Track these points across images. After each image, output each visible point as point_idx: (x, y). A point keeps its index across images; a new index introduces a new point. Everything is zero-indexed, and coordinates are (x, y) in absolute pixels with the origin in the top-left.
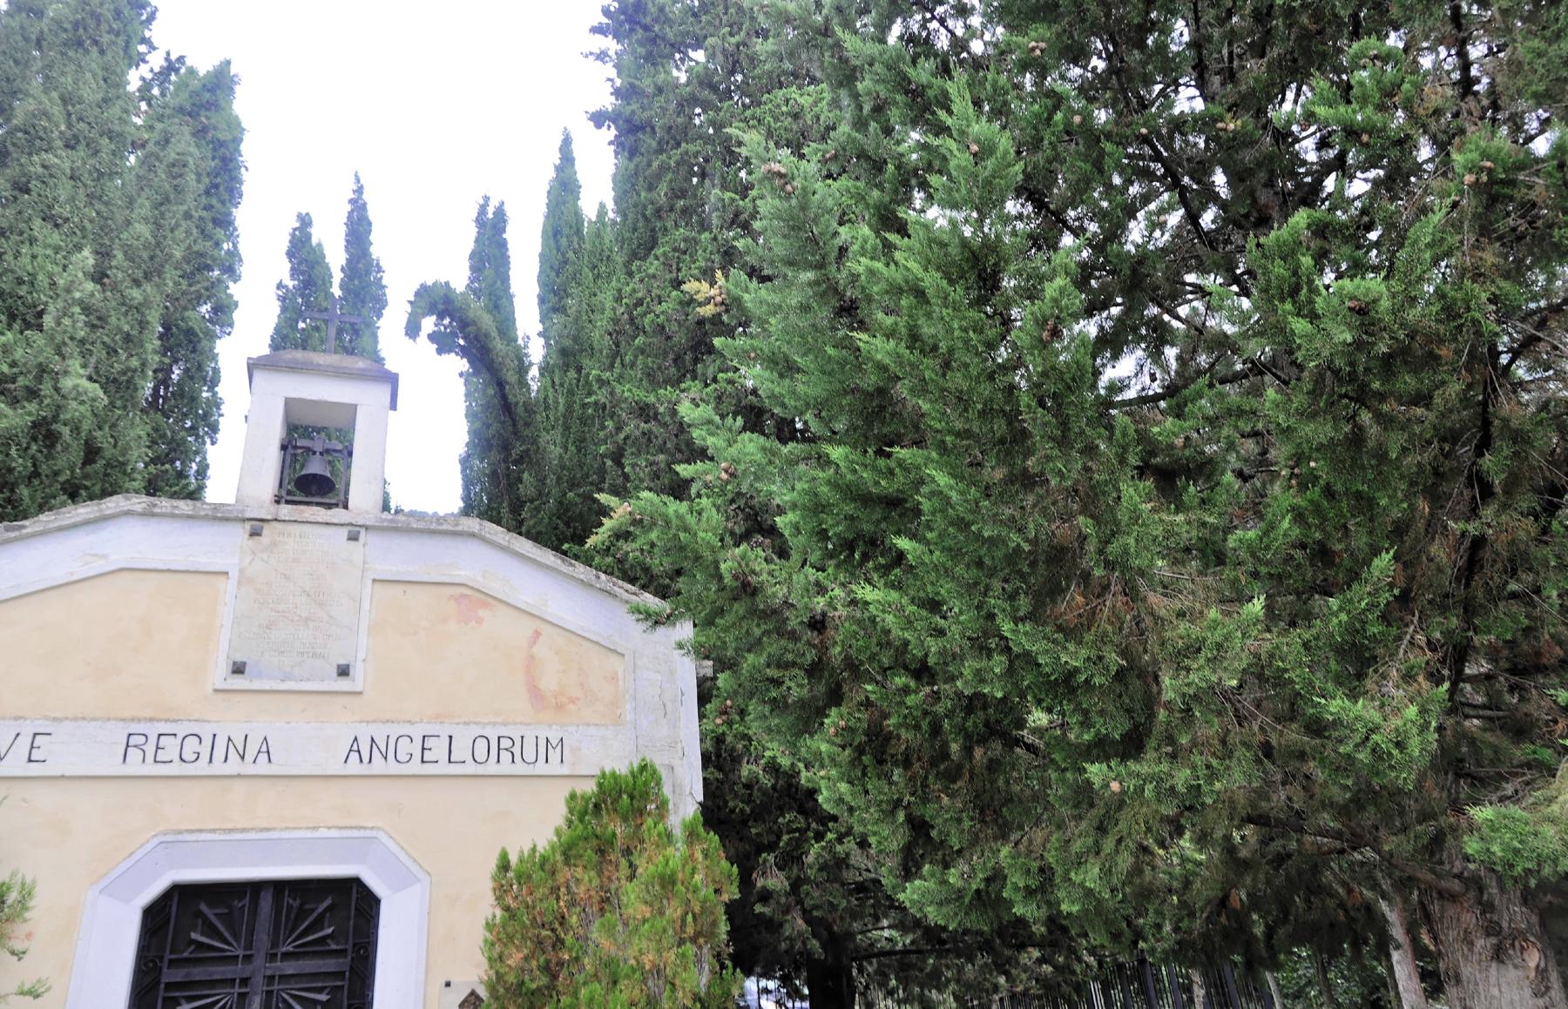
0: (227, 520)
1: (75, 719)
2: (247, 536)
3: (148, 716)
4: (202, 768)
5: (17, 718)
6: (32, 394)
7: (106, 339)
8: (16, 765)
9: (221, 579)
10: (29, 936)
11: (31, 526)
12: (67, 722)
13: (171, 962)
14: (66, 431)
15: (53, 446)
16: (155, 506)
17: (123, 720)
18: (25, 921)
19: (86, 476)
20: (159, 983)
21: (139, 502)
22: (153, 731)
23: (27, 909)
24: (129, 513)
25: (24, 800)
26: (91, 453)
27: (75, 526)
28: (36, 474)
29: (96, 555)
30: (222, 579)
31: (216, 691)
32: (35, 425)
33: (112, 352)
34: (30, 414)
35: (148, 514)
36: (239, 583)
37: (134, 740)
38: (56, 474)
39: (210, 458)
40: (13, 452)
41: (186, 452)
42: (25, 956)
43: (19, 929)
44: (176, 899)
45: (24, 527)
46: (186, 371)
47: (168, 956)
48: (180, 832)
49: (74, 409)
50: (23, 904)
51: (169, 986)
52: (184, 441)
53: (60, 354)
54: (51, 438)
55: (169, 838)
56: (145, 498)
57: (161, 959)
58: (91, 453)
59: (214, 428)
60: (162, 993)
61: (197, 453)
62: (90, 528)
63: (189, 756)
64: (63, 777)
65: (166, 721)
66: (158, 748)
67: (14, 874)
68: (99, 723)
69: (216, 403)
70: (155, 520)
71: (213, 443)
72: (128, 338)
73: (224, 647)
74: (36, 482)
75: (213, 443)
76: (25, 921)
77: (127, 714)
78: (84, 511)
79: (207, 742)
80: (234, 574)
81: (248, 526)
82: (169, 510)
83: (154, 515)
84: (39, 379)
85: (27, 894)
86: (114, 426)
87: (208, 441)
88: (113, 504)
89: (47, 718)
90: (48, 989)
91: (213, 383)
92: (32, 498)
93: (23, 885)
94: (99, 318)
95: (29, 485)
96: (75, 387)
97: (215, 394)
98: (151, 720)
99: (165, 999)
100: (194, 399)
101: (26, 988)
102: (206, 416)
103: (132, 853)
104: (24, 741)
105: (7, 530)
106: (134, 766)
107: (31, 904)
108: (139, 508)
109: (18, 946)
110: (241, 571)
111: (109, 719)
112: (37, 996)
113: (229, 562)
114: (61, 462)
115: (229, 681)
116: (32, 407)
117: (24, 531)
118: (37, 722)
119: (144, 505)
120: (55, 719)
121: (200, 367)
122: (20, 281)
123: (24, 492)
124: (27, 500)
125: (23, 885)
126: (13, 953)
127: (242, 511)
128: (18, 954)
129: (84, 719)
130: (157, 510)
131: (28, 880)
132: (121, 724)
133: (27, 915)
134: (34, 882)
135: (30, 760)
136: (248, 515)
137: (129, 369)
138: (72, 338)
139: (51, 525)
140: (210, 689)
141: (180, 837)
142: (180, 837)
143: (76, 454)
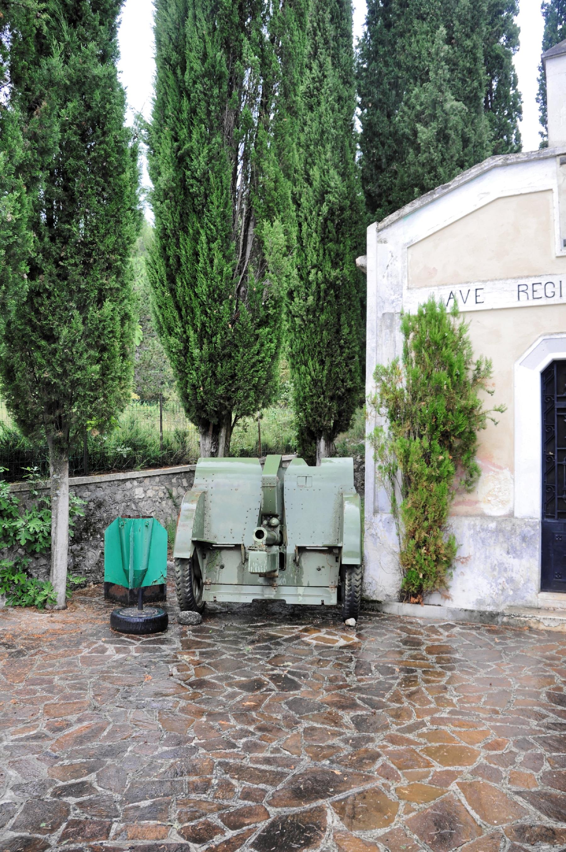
0: (546, 158)
1: (492, 280)
2: (559, 165)
3: (526, 274)
4: (556, 300)
5: (467, 283)
6: (434, 117)
7: (460, 75)
8: (471, 305)
9: (548, 195)
10: (493, 384)
11: (452, 184)
12: (489, 282)
13: (558, 398)
14: (452, 132)
15: (447, 143)
16: (508, 159)
17: (514, 278)
18: (491, 378)
19: (466, 155)
20: (554, 408)
21: (499, 159)
22: (529, 282)
23: (490, 372)
24: (495, 167)
25: (478, 322)
26: (466, 141)
27: (471, 180)
28: (444, 160)
29: (485, 193)
30: (549, 193)
31: (557, 257)
32: (438, 133)
33: (464, 81)
34: (434, 128)
35: (505, 165)
36: (559, 194)
37: (522, 288)
38: (452, 157)
39: (521, 131)
40: (432, 151)
41: (508, 130)
42: (494, 394)
43: (488, 381)
44: (555, 369)
45: (449, 186)
46: (499, 82)
47: (556, 396)
48: (552, 334)
49: (454, 119)
50: (488, 370)
51: (559, 410)
52: (506, 123)
53: (441, 91)
54: (446, 138)
55: (548, 337)
56: (501, 157)
57: (553, 396)
58: (466, 141)
59: (520, 111)
60: (556, 413)
61: (514, 128)
62: (478, 179)
63: (549, 294)
64: (492, 309)
65: (535, 276)
66: (534, 291)
67: (481, 356)
68: (504, 281)
69: (518, 96)
70: (509, 167)
71: (521, 120)
72: (470, 71)
73: (557, 232)
74: (444, 163)
75: (521, 120)
76: (491, 378)
77: (515, 275)
78: (474, 171)
79: (557, 285)
80: (555, 190)
81: (558, 159)
82: (515, 160)
83: (508, 165)
84: (434, 108)
85: (489, 366)
86: (472, 122)
87: (518, 119)
88: (488, 163)
89: (479, 281)
90: (506, 409)
91: (515, 83)
92: (445, 172)
93: (486, 361)
94: (454, 65)
95: (442, 166)
96: (452, 107)
97: (516, 90)
98: (527, 277)
99: (558, 416)
100: (506, 96)
101: (497, 408)
102: (515, 104)
103: (531, 346)
104: (472, 293)
105: (443, 188)
106: (524, 302)
107: (492, 370)
108: (500, 163)
109: (490, 389)
110: (559, 187)
111: (507, 279)
112: (502, 412)
113: (552, 184)
114: (453, 151)
115: (563, 251)
116: (434, 124)
117: (452, 187)
118: (476, 284)
119: (502, 160)
120: (483, 281)
121: (506, 77)
122: (415, 58)
123: (440, 170)
124: (443, 174)
125: (486, 361)
126: (489, 392)
127: (554, 151)
128: (491, 393)
129: (496, 280)
130: (509, 162)
131: (488, 359)
132: (513, 281)
133: (491, 375)
134: (491, 359)
135: (477, 303)
136: (557, 153)
137: (474, 89)
138: (444, 80)
139: (461, 182)
140: (554, 257)
141: (552, 337)
142: (552, 337)
143: (459, 144)
